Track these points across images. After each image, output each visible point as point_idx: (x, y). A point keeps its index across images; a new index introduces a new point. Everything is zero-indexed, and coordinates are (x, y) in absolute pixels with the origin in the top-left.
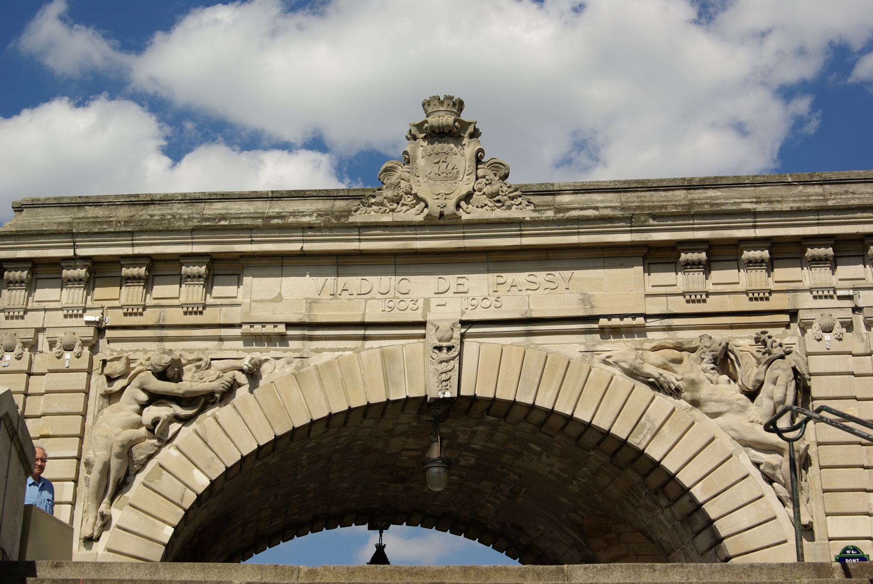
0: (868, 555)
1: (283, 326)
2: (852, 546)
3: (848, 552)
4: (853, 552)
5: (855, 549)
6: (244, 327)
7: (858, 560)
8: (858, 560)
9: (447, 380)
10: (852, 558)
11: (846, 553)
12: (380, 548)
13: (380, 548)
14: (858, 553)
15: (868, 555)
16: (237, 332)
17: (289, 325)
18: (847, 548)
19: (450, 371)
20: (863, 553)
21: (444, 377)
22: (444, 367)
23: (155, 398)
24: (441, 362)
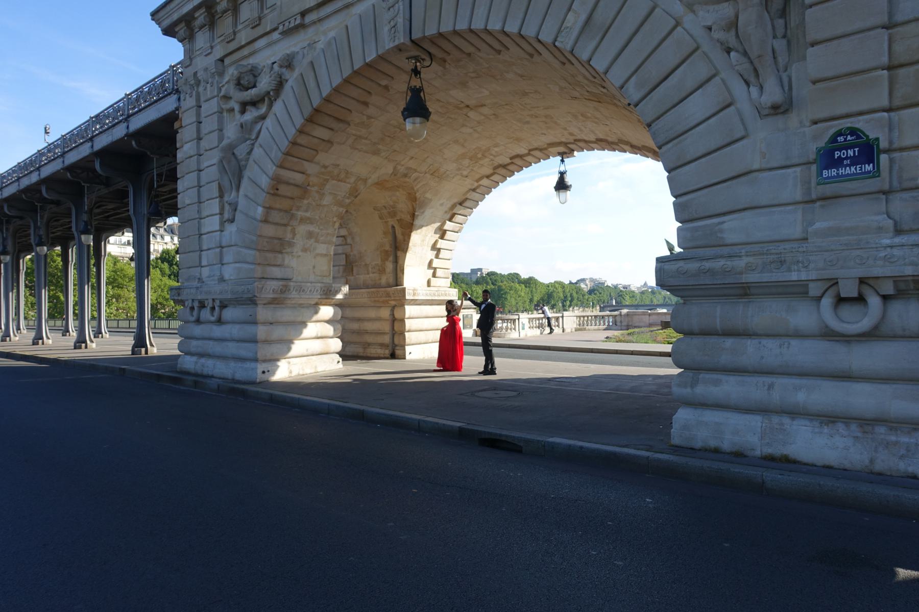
0: (877, 139)
1: (299, 17)
2: (848, 128)
3: (841, 139)
4: (849, 138)
5: (853, 132)
6: (281, 27)
7: (856, 149)
8: (856, 149)
9: (394, 27)
10: (847, 148)
11: (837, 141)
12: (562, 174)
13: (562, 174)
14: (859, 137)
15: (877, 139)
16: (276, 35)
17: (303, 14)
18: (839, 133)
19: (396, 16)
20: (867, 136)
21: (392, 24)
22: (392, 13)
23: (244, 106)
24: (389, 9)
